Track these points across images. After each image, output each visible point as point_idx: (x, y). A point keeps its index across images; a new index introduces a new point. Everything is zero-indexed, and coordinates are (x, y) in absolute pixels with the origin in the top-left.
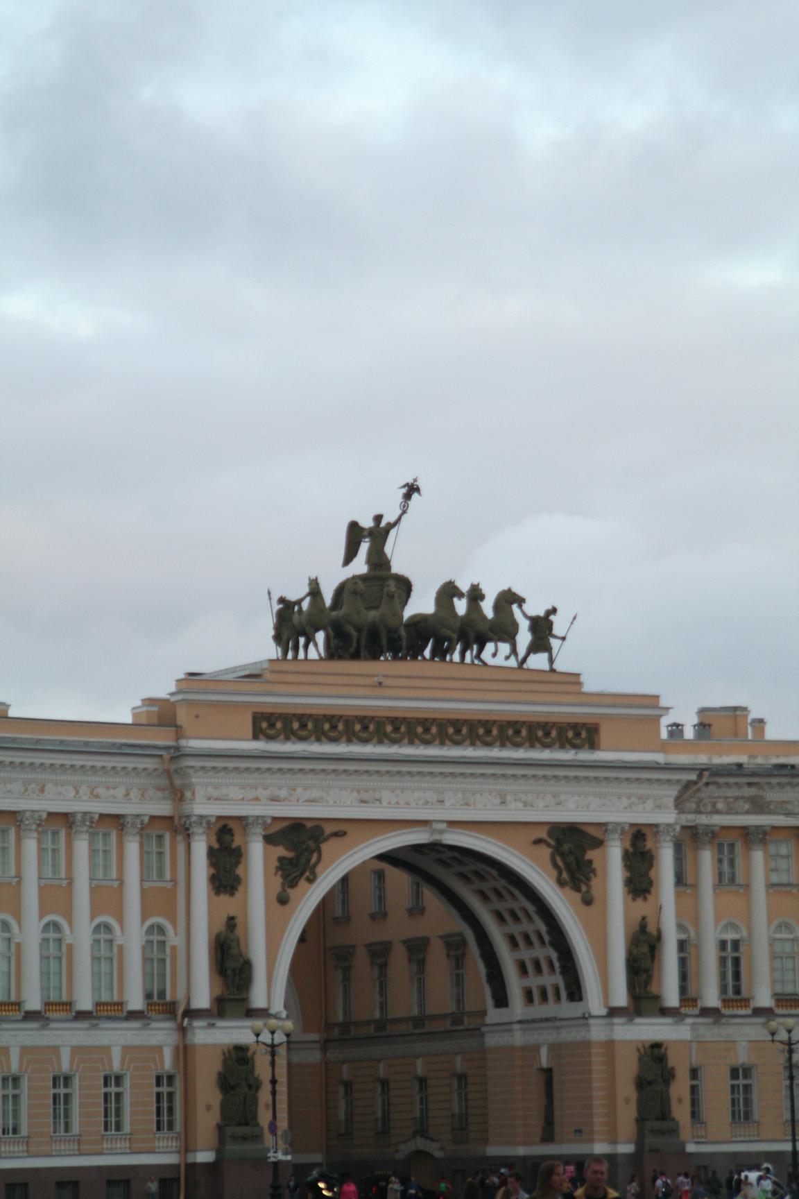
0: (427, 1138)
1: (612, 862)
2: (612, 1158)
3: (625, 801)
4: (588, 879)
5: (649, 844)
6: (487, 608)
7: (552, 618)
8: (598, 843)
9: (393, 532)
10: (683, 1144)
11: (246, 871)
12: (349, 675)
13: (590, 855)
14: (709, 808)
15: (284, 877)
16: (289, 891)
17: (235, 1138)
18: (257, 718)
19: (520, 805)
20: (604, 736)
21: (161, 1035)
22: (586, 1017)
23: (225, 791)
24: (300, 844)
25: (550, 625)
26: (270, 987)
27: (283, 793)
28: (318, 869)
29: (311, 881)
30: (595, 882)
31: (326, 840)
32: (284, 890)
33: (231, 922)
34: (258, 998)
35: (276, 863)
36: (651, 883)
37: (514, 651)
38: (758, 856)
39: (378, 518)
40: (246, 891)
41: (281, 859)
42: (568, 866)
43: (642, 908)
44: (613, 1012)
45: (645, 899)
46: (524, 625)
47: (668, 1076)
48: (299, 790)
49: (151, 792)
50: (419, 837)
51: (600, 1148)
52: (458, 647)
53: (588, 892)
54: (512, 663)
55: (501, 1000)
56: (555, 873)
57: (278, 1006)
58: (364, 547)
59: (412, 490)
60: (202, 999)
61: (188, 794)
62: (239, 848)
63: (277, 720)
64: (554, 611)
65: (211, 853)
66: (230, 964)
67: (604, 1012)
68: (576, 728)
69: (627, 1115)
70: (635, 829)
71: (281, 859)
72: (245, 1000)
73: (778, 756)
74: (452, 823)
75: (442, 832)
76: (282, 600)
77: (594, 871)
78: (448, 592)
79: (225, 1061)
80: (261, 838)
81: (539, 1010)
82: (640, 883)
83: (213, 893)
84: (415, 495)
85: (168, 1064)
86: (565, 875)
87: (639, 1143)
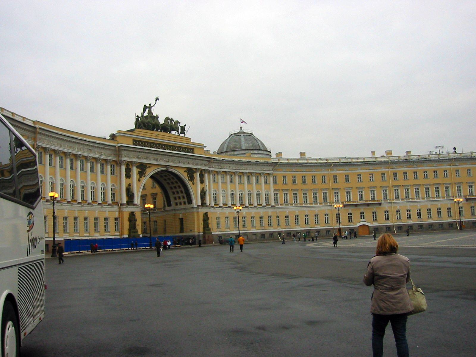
0: (147, 233)
1: (197, 176)
2: (199, 236)
5: (203, 173)
6: (173, 122)
7: (185, 127)
8: (195, 172)
9: (152, 108)
10: (211, 233)
11: (132, 173)
14: (212, 167)
15: (139, 175)
17: (133, 232)
18: (134, 140)
19: (182, 163)
20: (195, 151)
21: (116, 208)
22: (193, 208)
24: (142, 168)
28: (146, 174)
29: (144, 177)
30: (194, 180)
31: (147, 168)
33: (129, 185)
35: (138, 172)
36: (203, 181)
37: (178, 132)
38: (220, 177)
39: (150, 105)
40: (132, 178)
41: (139, 171)
43: (203, 186)
44: (198, 206)
45: (203, 184)
46: (180, 128)
47: (208, 219)
49: (113, 155)
50: (164, 169)
51: (196, 234)
53: (193, 182)
54: (178, 135)
55: (169, 205)
57: (139, 203)
58: (147, 110)
59: (157, 99)
60: (124, 201)
61: (121, 156)
62: (130, 168)
65: (125, 169)
66: (130, 194)
67: (196, 206)
68: (191, 149)
69: (202, 226)
71: (139, 171)
72: (133, 202)
75: (168, 168)
76: (137, 116)
77: (194, 178)
78: (167, 119)
79: (130, 215)
81: (179, 207)
84: (158, 100)
85: (117, 215)
87: (204, 233)
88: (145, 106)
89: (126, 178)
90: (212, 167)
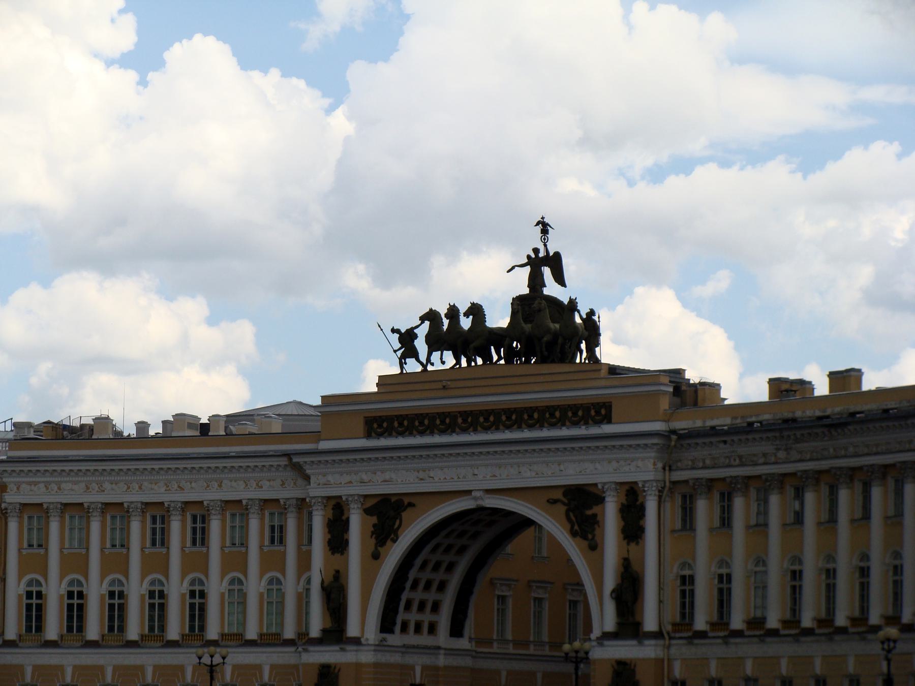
3: (614, 464)
4: (594, 530)
5: (640, 500)
8: (600, 500)
12: (474, 379)
13: (596, 510)
15: (376, 538)
16: (379, 549)
23: (330, 478)
25: (595, 322)
26: (362, 620)
27: (365, 477)
29: (394, 541)
31: (405, 510)
32: (376, 548)
34: (353, 630)
36: (642, 530)
39: (536, 251)
41: (374, 526)
42: (576, 517)
45: (637, 543)
48: (379, 473)
52: (583, 346)
53: (593, 538)
56: (568, 526)
57: (371, 634)
59: (545, 227)
63: (556, 410)
64: (592, 313)
70: (627, 487)
71: (374, 526)
73: (751, 416)
74: (488, 491)
76: (394, 331)
77: (597, 523)
80: (361, 511)
82: (632, 531)
83: (330, 553)
86: (576, 527)
88: (529, 257)
89: (333, 553)
90: (701, 465)
